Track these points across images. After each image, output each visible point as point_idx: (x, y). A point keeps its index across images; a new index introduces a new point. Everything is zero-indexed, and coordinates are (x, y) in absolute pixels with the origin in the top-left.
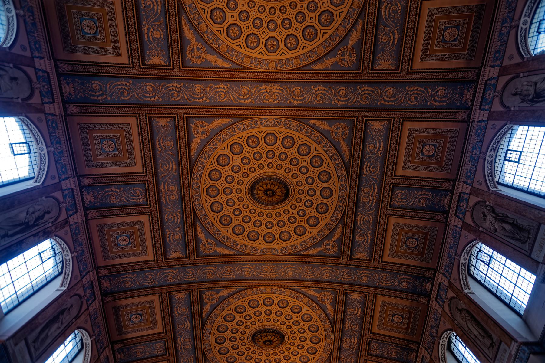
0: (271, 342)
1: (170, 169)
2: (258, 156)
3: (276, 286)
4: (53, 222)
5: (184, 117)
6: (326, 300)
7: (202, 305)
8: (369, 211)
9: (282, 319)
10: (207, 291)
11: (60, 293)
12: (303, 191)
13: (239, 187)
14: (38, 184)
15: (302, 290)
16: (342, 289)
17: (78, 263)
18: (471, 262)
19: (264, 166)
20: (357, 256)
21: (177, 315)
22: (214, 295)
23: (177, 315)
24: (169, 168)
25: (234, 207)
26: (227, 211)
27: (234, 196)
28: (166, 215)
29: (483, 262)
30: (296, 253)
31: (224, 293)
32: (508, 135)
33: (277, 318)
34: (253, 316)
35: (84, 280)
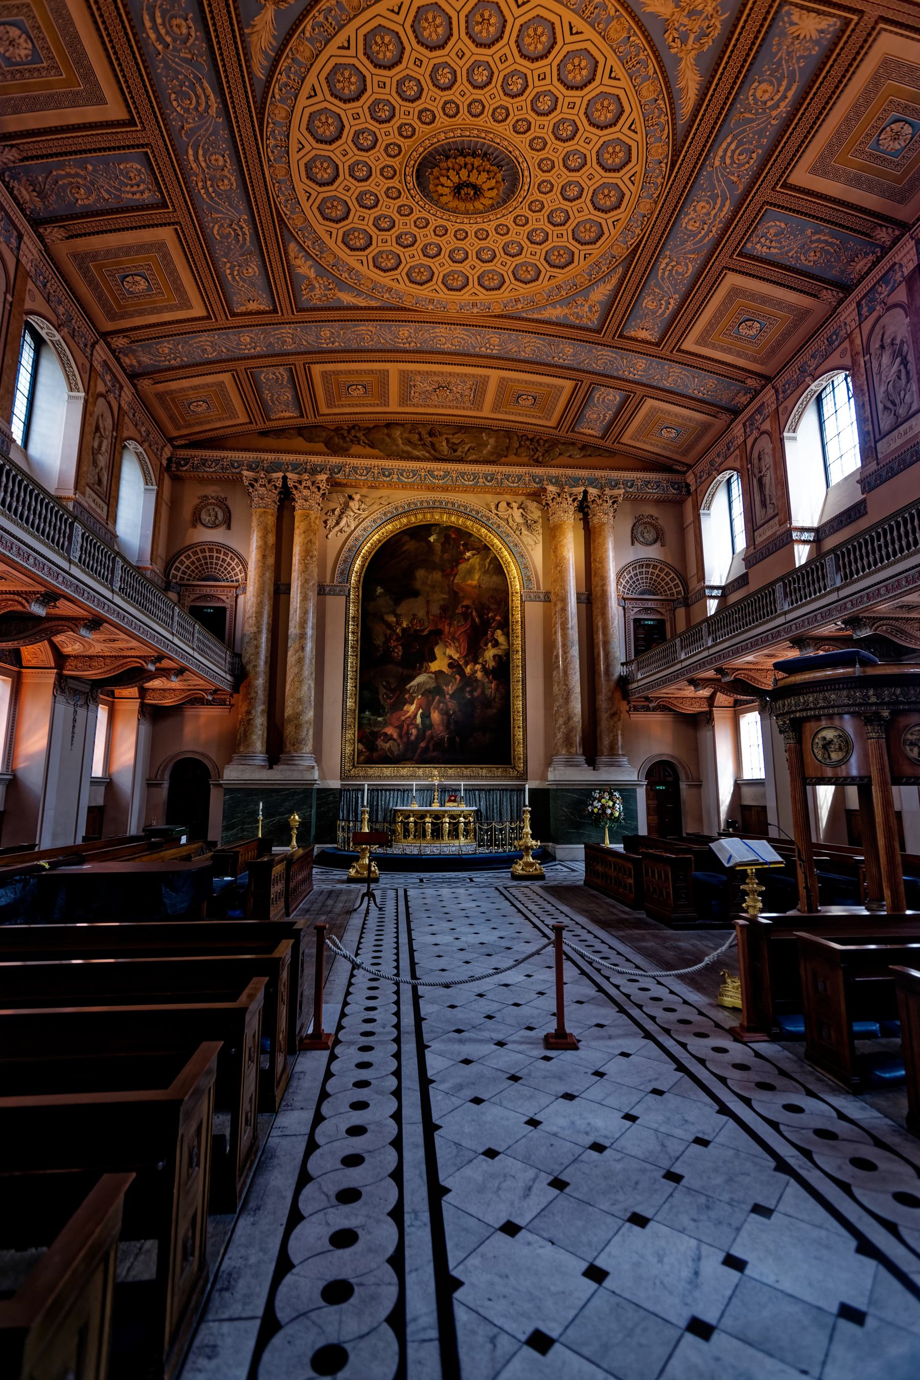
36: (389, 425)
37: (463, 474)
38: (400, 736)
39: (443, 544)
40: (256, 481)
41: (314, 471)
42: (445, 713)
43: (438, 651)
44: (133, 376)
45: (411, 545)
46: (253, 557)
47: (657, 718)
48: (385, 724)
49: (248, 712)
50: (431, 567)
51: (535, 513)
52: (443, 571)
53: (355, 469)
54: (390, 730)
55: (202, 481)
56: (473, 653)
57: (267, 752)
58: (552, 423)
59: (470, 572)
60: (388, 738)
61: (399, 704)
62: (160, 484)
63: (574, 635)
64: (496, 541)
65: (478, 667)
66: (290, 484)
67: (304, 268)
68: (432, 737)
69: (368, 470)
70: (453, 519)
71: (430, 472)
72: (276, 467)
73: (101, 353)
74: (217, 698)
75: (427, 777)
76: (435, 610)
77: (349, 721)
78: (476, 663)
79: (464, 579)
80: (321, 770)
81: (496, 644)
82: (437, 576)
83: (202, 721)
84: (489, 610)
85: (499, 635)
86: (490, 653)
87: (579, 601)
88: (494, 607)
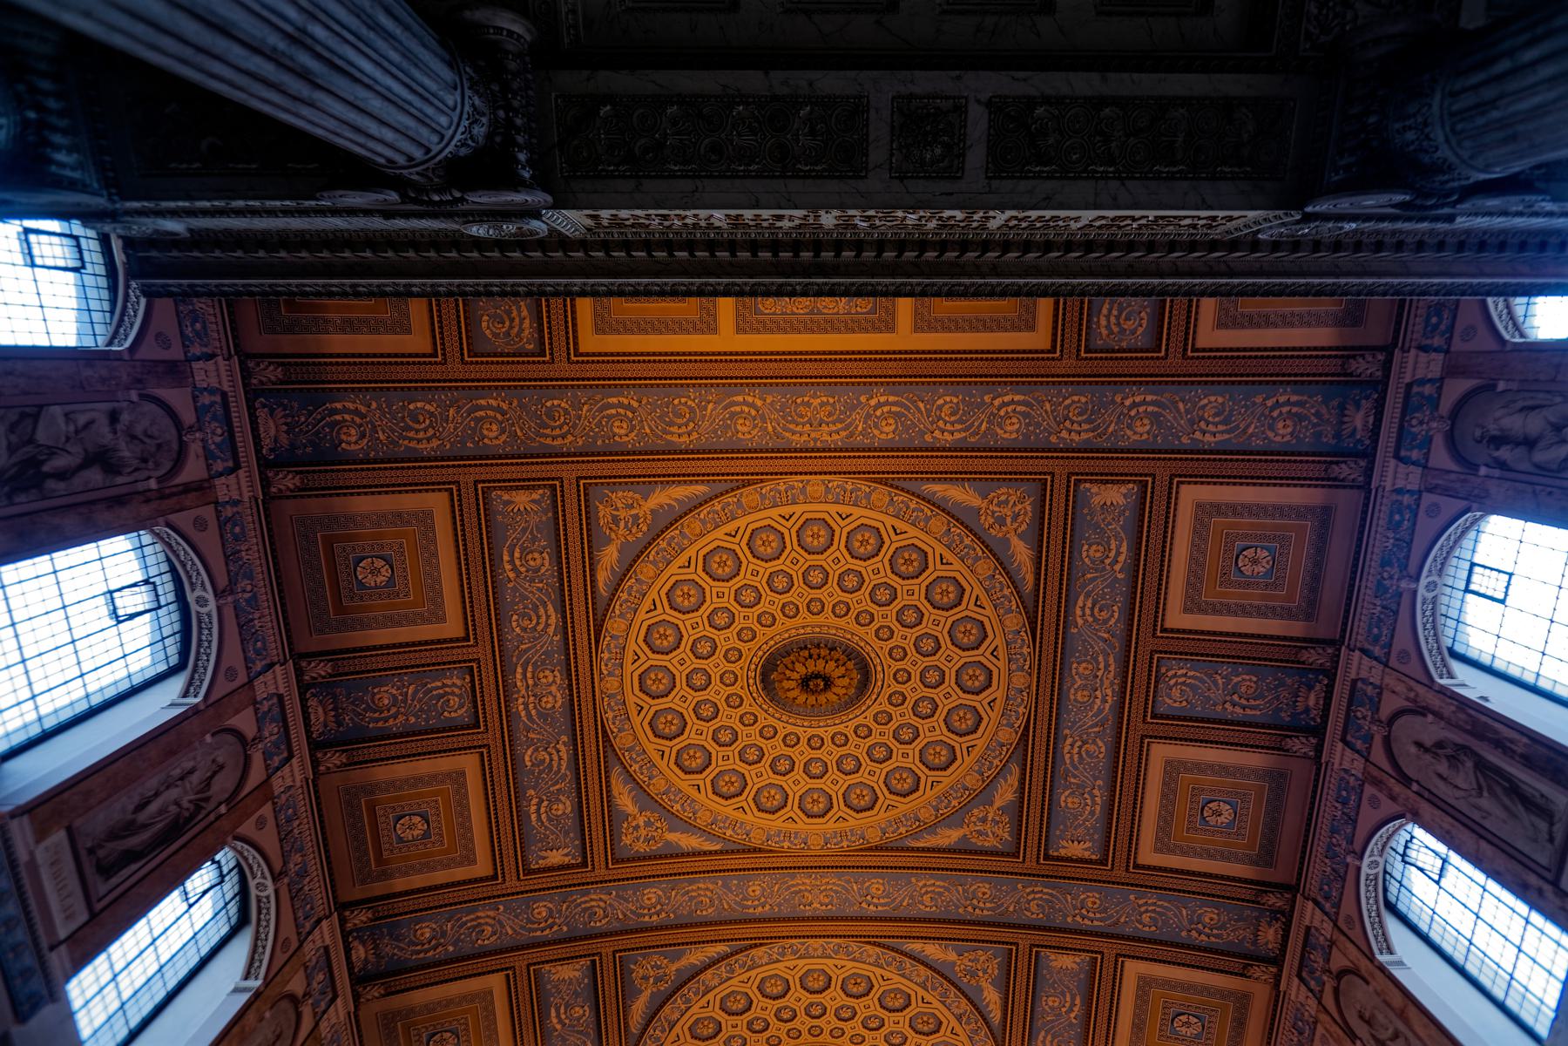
1: (540, 628)
2: (780, 583)
3: (836, 936)
4: (227, 801)
5: (578, 486)
6: (980, 974)
7: (626, 993)
8: (1092, 727)
10: (641, 955)
11: (244, 997)
12: (909, 674)
13: (731, 667)
14: (192, 700)
15: (915, 946)
16: (1024, 944)
17: (292, 899)
18: (1389, 869)
19: (798, 609)
20: (1063, 852)
21: (558, 1027)
22: (659, 967)
23: (558, 1027)
24: (538, 623)
25: (716, 724)
26: (697, 734)
27: (718, 693)
28: (529, 752)
29: (1422, 870)
30: (894, 845)
31: (695, 957)
32: (1472, 534)
33: (841, 1024)
34: (773, 1020)
35: (308, 946)
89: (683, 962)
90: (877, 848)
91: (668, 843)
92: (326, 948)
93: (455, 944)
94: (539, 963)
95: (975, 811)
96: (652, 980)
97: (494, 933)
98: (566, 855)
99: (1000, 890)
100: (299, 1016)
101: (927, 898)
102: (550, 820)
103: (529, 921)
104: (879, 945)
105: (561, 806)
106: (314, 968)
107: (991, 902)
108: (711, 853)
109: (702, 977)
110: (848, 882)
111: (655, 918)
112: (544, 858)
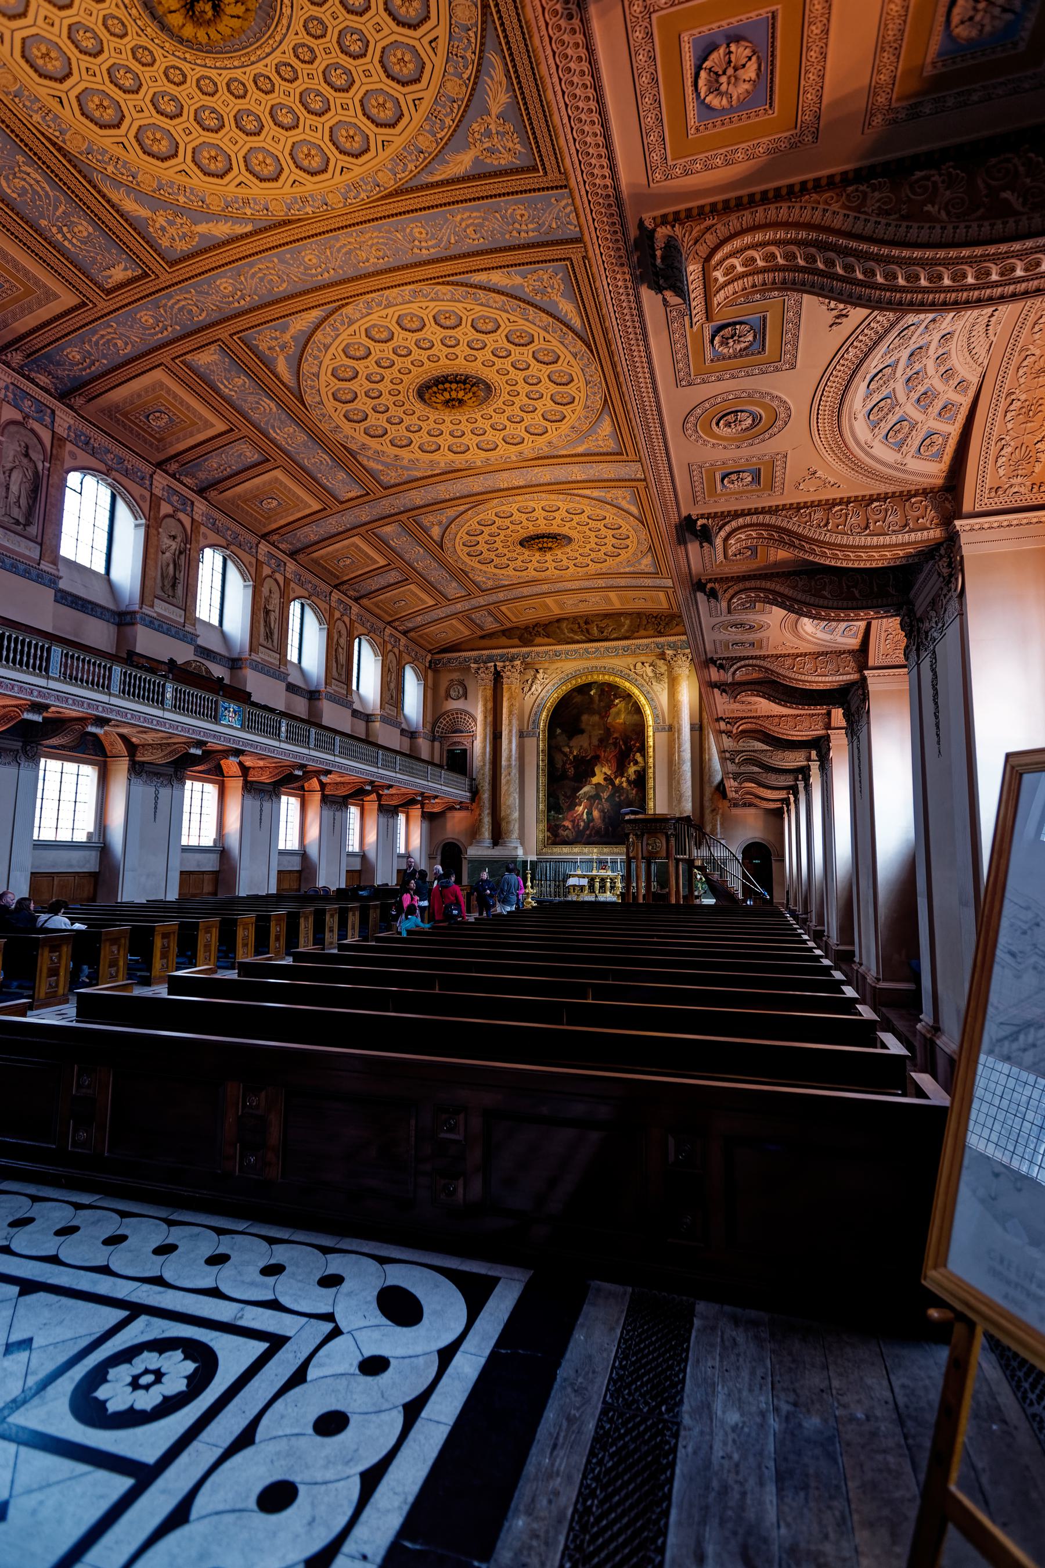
0: (461, 402)
6: (549, 290)
9: (462, 350)
36: (558, 621)
37: (607, 649)
38: (573, 827)
39: (600, 696)
40: (479, 669)
41: (512, 659)
42: (602, 811)
43: (597, 770)
44: (405, 633)
45: (578, 699)
46: (480, 717)
47: (751, 811)
48: (564, 819)
49: (480, 815)
50: (592, 712)
51: (663, 667)
52: (600, 714)
53: (538, 653)
54: (567, 823)
55: (450, 671)
56: (621, 770)
57: (493, 838)
58: (665, 605)
59: (618, 713)
60: (566, 828)
61: (573, 805)
62: (426, 680)
63: (687, 754)
64: (636, 692)
65: (624, 779)
66: (499, 669)
67: (479, 579)
68: (593, 827)
69: (546, 653)
70: (606, 677)
71: (586, 650)
72: (490, 659)
73: (388, 630)
74: (463, 807)
75: (589, 853)
76: (595, 742)
77: (541, 816)
78: (622, 776)
79: (614, 719)
80: (524, 849)
81: (636, 763)
82: (596, 718)
83: (456, 820)
84: (632, 739)
85: (638, 757)
86: (632, 769)
87: (692, 728)
88: (634, 737)
89: (292, 331)
90: (397, 192)
91: (202, 236)
92: (12, 383)
93: (104, 357)
94: (182, 355)
95: (475, 125)
96: (277, 348)
97: (126, 344)
98: (125, 269)
99: (536, 208)
100: (32, 430)
101: (470, 230)
102: (82, 242)
103: (145, 329)
104: (448, 283)
105: (80, 228)
106: (15, 399)
107: (532, 222)
108: (247, 235)
109: (315, 338)
110: (389, 232)
111: (242, 302)
112: (110, 277)
